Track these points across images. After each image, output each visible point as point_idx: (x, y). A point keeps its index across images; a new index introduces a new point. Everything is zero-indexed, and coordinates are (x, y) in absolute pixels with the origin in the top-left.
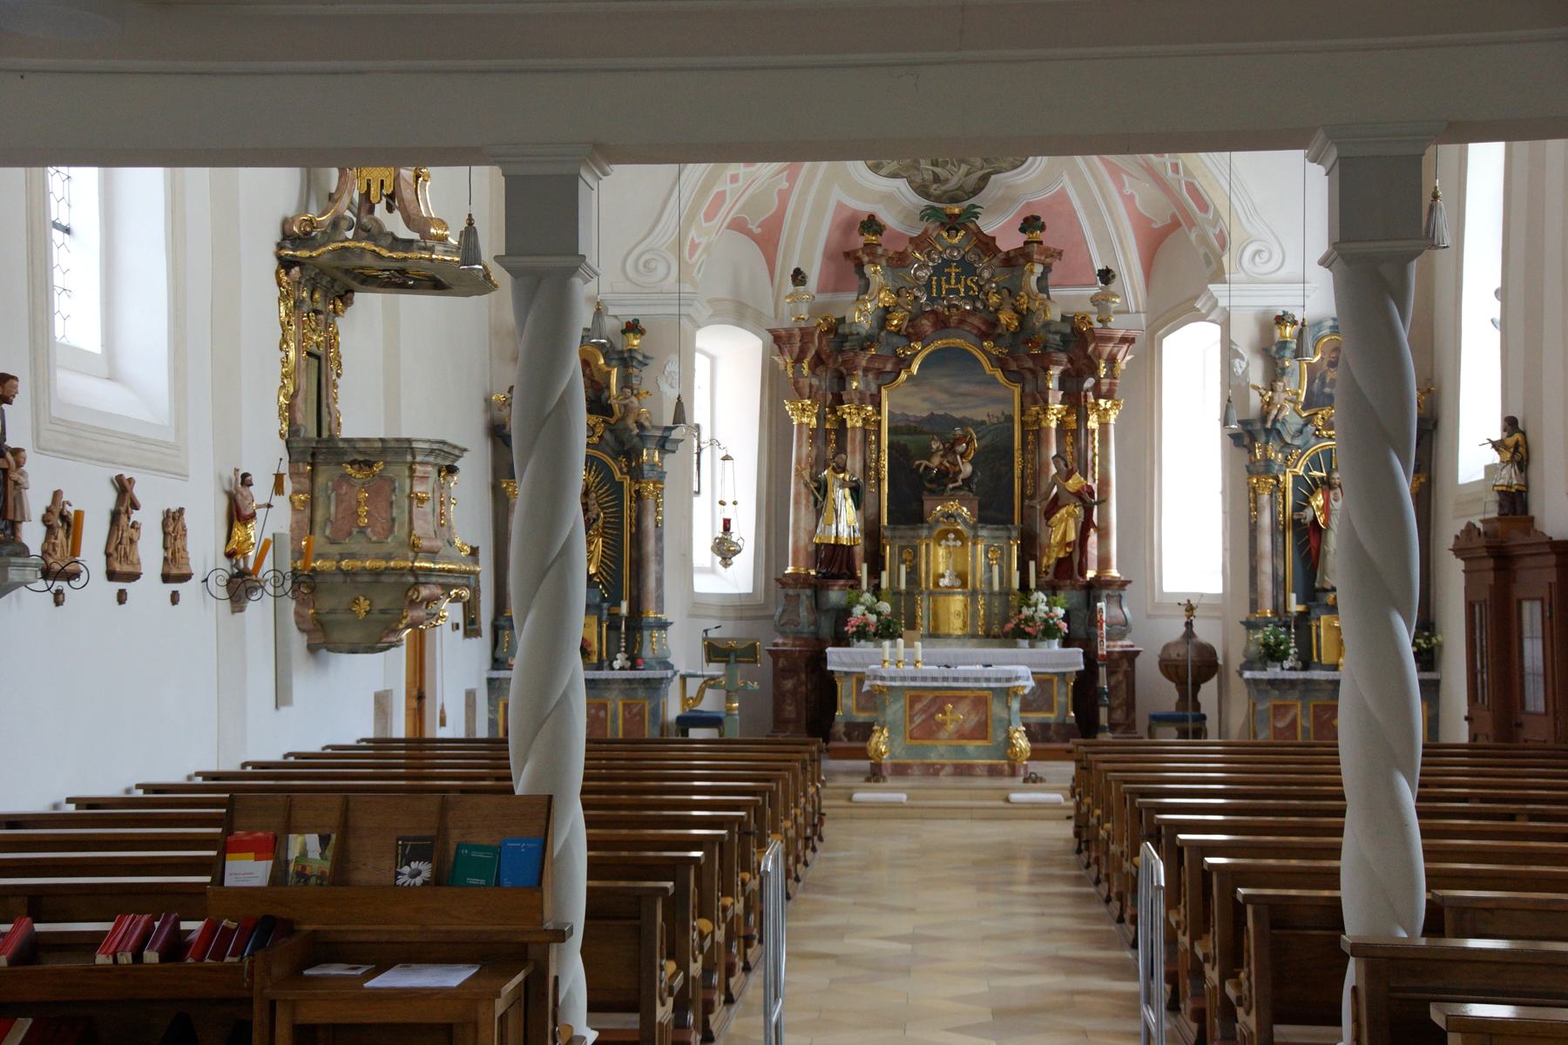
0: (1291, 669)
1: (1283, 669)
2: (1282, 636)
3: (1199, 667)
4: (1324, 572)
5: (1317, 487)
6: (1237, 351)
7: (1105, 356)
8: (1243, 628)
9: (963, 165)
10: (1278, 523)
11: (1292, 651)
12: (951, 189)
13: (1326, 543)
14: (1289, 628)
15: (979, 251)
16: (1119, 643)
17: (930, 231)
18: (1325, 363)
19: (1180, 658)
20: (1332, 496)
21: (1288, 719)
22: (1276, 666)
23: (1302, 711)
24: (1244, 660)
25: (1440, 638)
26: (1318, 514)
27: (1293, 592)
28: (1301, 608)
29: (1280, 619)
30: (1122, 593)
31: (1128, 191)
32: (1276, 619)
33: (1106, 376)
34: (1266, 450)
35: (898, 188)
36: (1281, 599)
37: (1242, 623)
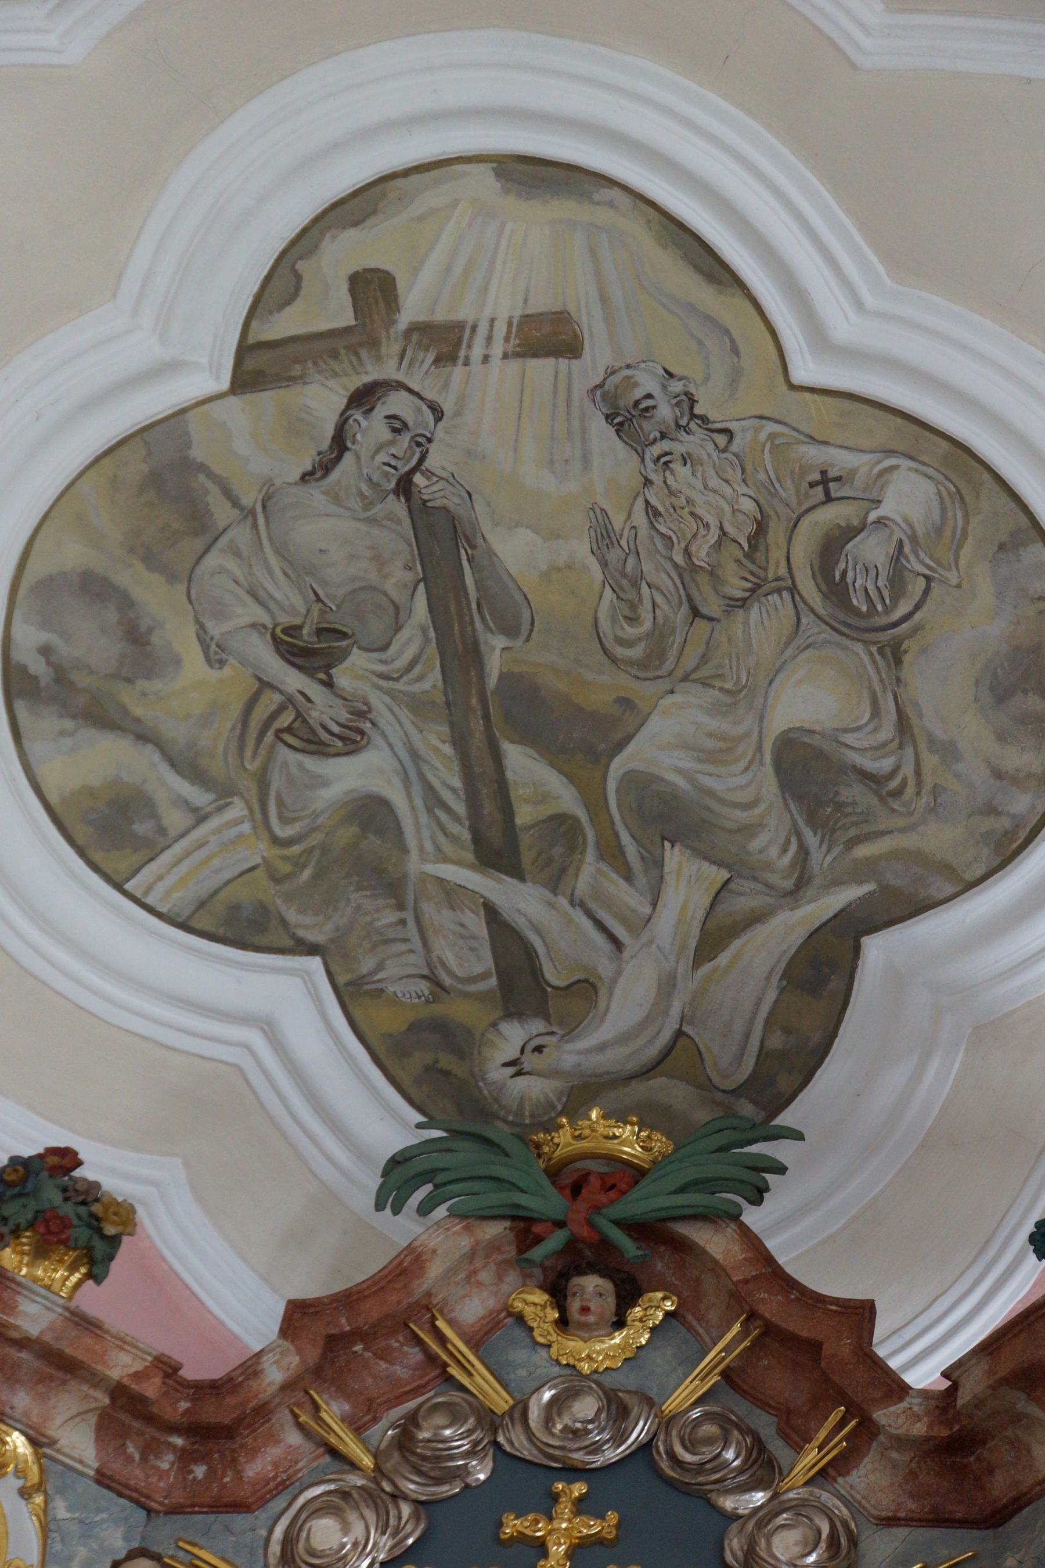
9: (674, 857)
12: (614, 1060)
15: (765, 1424)
17: (435, 1270)
35: (269, 1028)
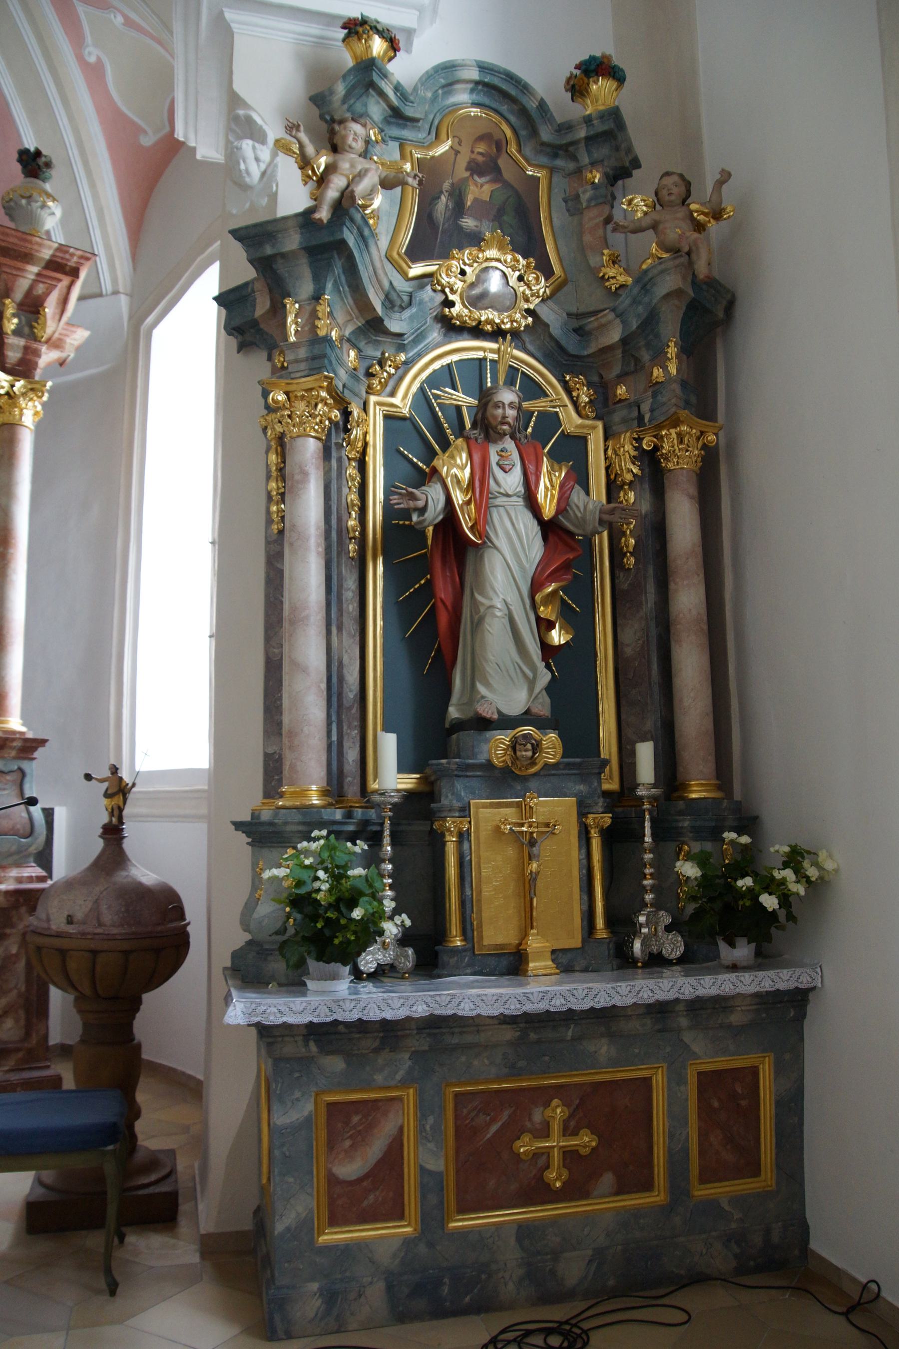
0: (380, 974)
1: (358, 975)
2: (358, 871)
3: (126, 953)
4: (475, 674)
5: (445, 445)
6: (249, 120)
7: (19, 294)
8: (242, 838)
10: (342, 530)
11: (391, 929)
13: (480, 583)
14: (375, 840)
16: (14, 873)
18: (462, 162)
19: (71, 929)
20: (494, 458)
21: (375, 1149)
22: (334, 977)
23: (422, 1116)
24: (248, 937)
25: (829, 865)
26: (458, 497)
27: (387, 729)
28: (408, 782)
29: (349, 815)
30: (25, 765)
31: (92, 54)
32: (338, 815)
33: (17, 332)
34: (314, 315)
36: (352, 755)
37: (239, 826)
